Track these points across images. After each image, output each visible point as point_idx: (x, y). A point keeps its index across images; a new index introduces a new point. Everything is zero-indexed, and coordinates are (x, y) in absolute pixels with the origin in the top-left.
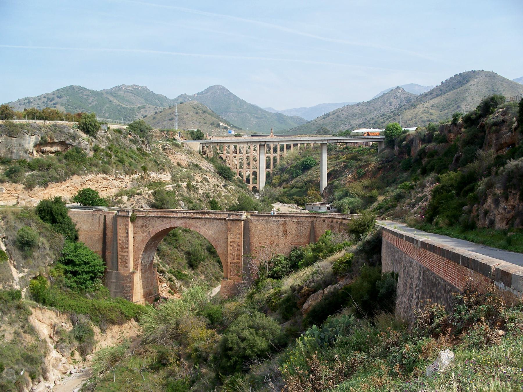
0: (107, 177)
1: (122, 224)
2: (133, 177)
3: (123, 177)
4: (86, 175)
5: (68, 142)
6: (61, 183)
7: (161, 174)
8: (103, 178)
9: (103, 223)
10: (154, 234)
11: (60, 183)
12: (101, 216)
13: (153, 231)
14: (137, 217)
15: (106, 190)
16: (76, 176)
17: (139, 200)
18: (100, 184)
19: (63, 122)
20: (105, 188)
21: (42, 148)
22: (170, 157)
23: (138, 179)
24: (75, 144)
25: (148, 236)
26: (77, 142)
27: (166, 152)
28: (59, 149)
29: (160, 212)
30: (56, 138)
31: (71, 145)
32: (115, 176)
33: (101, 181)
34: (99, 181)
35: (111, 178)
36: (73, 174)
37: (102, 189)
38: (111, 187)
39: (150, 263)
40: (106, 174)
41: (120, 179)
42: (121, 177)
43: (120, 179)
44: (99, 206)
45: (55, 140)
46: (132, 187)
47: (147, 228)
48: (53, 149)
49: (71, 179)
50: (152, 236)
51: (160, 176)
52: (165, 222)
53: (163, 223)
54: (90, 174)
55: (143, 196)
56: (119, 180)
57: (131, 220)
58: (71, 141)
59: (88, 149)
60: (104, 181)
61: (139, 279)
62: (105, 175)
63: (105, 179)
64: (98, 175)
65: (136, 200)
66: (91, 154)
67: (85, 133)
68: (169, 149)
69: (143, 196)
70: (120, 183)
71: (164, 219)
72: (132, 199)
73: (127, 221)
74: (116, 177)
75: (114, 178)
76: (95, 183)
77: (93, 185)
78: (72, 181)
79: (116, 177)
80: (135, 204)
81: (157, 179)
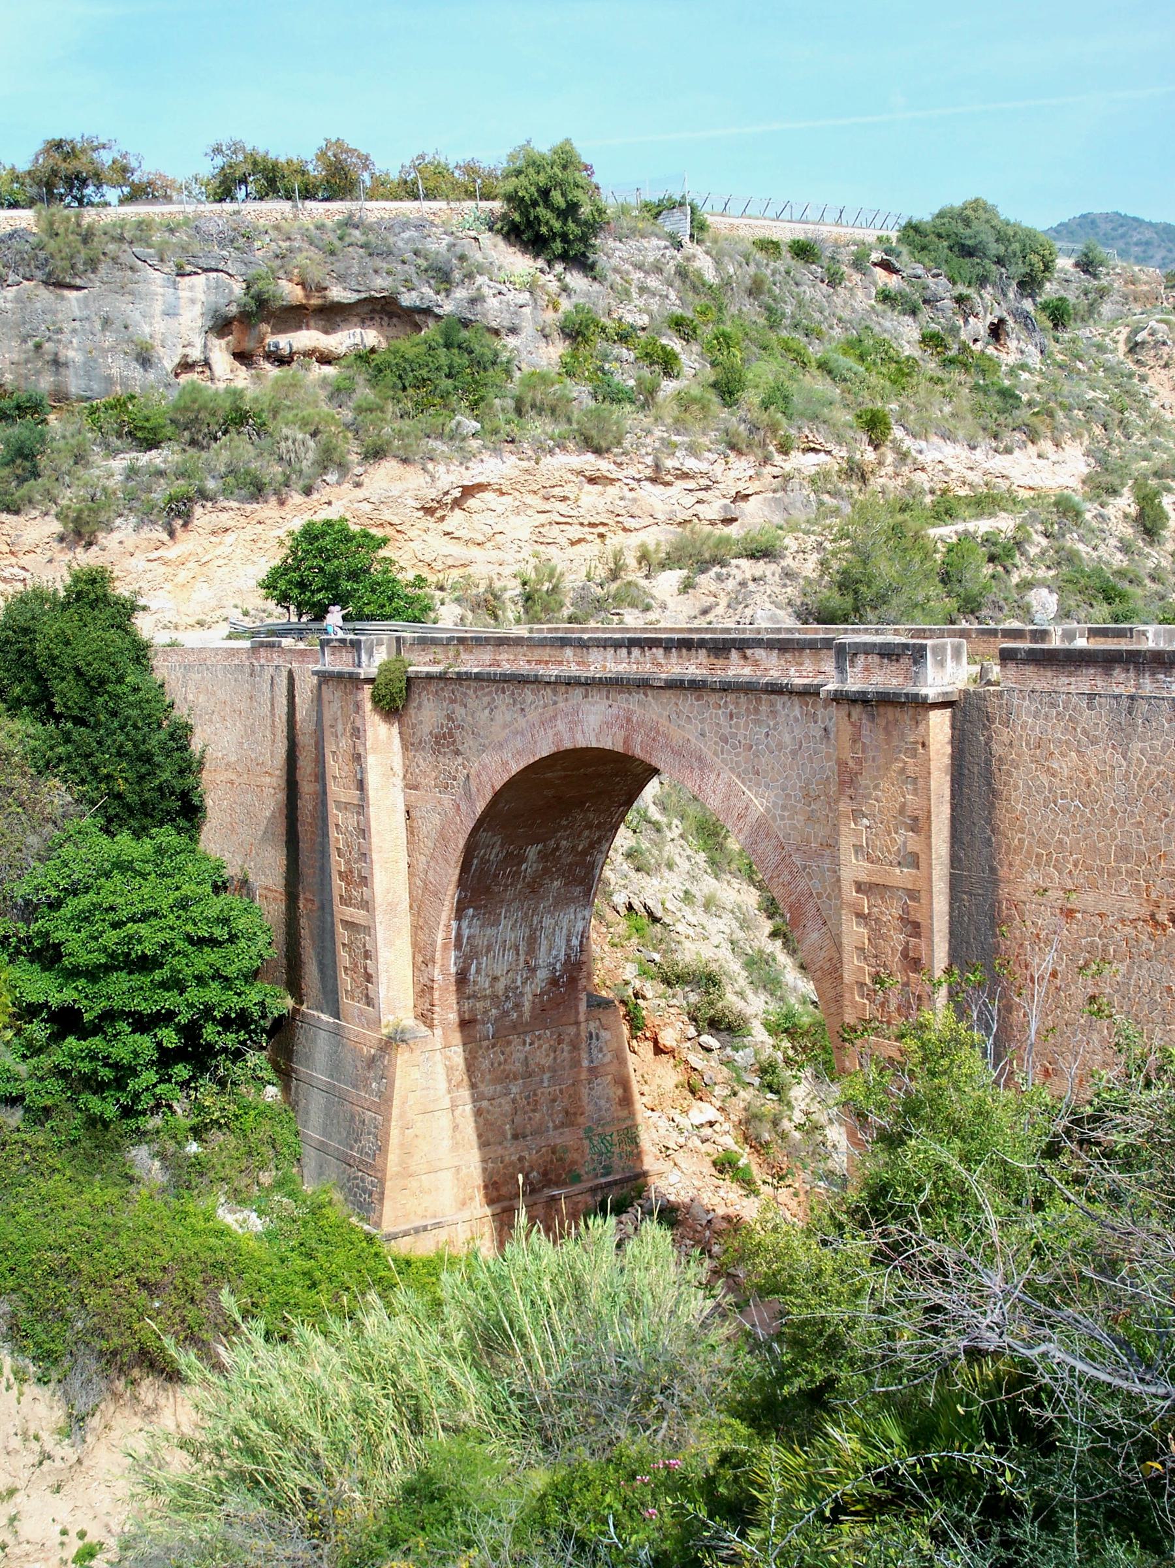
0: (604, 465)
1: (340, 727)
2: (788, 467)
3: (704, 466)
4: (466, 457)
5: (408, 299)
6: (282, 503)
7: (1008, 451)
8: (580, 473)
9: (284, 718)
10: (489, 797)
11: (273, 500)
12: (277, 680)
13: (484, 778)
14: (409, 679)
15: (601, 536)
16: (389, 466)
17: (752, 586)
18: (562, 507)
19: (416, 204)
20: (592, 525)
21: (270, 340)
22: (1152, 382)
23: (818, 481)
24: (448, 308)
25: (463, 807)
26: (460, 293)
27: (1138, 362)
28: (371, 337)
29: (668, 645)
30: (341, 278)
31: (427, 312)
32: (649, 460)
33: (569, 490)
34: (557, 491)
35: (631, 471)
36: (376, 454)
37: (575, 532)
38: (630, 523)
39: (554, 982)
40: (598, 451)
41: (685, 476)
42: (691, 464)
43: (685, 476)
44: (371, 618)
45: (338, 293)
46: (778, 519)
47: (457, 753)
48: (342, 340)
49: (358, 485)
50: (480, 807)
51: (1000, 463)
52: (533, 715)
53: (522, 722)
54: (497, 452)
55: (788, 562)
56: (681, 484)
57: (376, 700)
58: (426, 290)
59: (528, 329)
60: (588, 487)
61: (443, 1085)
62: (590, 457)
63: (592, 481)
64: (547, 460)
65: (731, 584)
66: (555, 352)
67: (524, 253)
68: (1157, 342)
69: (788, 562)
70: (690, 500)
71: (528, 694)
72: (706, 581)
73: (358, 707)
74: (657, 467)
75: (648, 472)
76: (530, 499)
77: (517, 511)
78: (360, 493)
79: (657, 467)
80: (720, 610)
81: (971, 476)
